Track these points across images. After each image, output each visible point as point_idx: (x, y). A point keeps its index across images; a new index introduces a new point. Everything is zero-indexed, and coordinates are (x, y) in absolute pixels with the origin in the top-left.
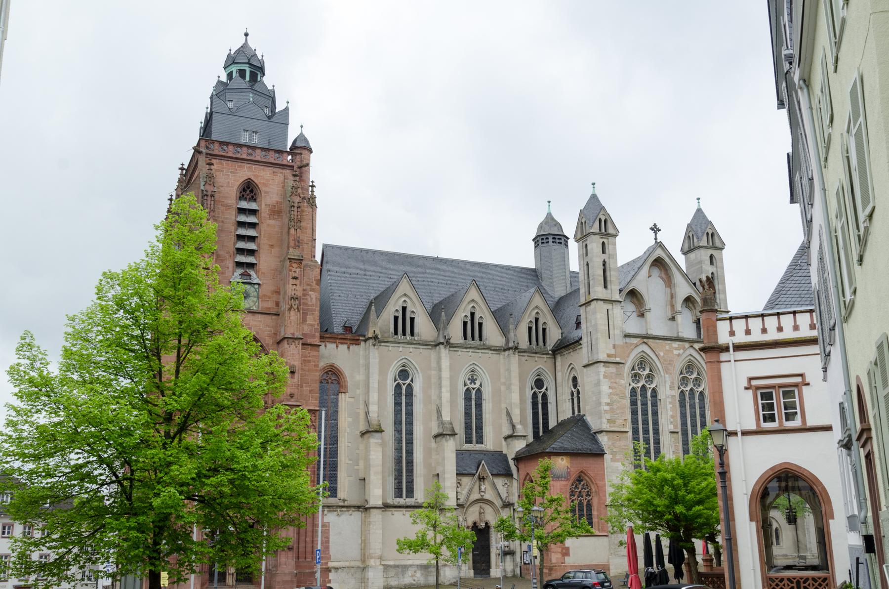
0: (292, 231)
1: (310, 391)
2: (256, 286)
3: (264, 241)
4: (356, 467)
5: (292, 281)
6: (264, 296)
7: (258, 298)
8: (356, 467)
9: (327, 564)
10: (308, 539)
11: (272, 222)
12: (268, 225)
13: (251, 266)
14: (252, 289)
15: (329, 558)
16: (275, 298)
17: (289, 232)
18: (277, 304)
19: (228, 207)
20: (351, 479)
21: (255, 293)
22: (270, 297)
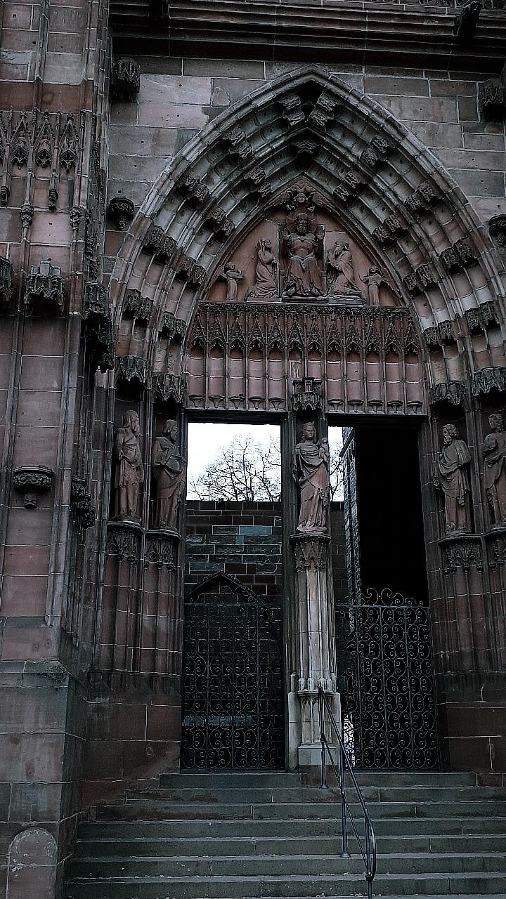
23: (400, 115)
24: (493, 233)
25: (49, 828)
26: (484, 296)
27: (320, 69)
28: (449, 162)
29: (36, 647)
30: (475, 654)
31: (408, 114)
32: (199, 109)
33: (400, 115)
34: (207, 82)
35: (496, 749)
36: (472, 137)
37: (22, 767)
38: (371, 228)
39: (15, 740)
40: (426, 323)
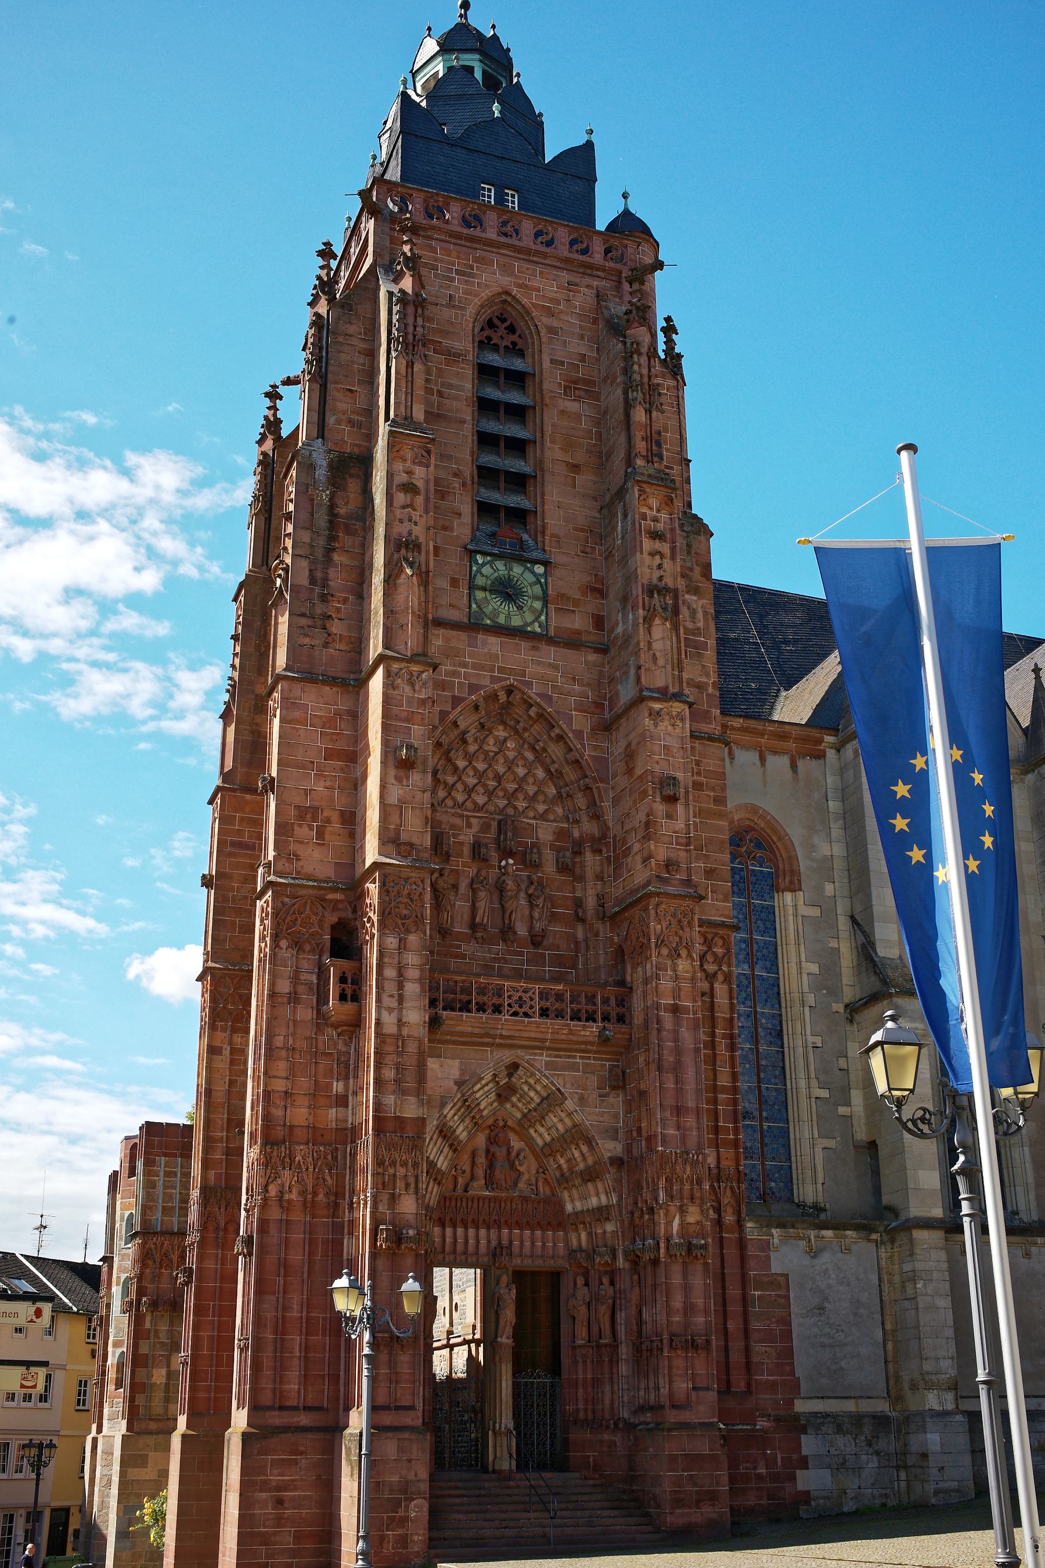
0: (639, 415)
1: (709, 873)
2: (540, 569)
3: (553, 453)
4: (842, 1110)
5: (647, 544)
6: (562, 596)
7: (545, 600)
8: (842, 1110)
9: (790, 1403)
10: (731, 1325)
11: (572, 406)
12: (563, 412)
13: (519, 516)
14: (529, 577)
15: (794, 1388)
16: (592, 605)
17: (627, 415)
18: (599, 622)
19: (453, 356)
20: (831, 1143)
21: (537, 590)
22: (577, 603)
23: (564, 1086)
24: (611, 1164)
25: (425, 1498)
26: (604, 1200)
27: (520, 1052)
28: (589, 1118)
29: (413, 1420)
30: (586, 1410)
31: (568, 1085)
32: (452, 1083)
33: (564, 1086)
34: (456, 1063)
35: (594, 1460)
36: (603, 1101)
37: (413, 1473)
38: (540, 1142)
39: (409, 1461)
40: (569, 1208)
